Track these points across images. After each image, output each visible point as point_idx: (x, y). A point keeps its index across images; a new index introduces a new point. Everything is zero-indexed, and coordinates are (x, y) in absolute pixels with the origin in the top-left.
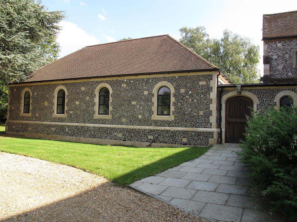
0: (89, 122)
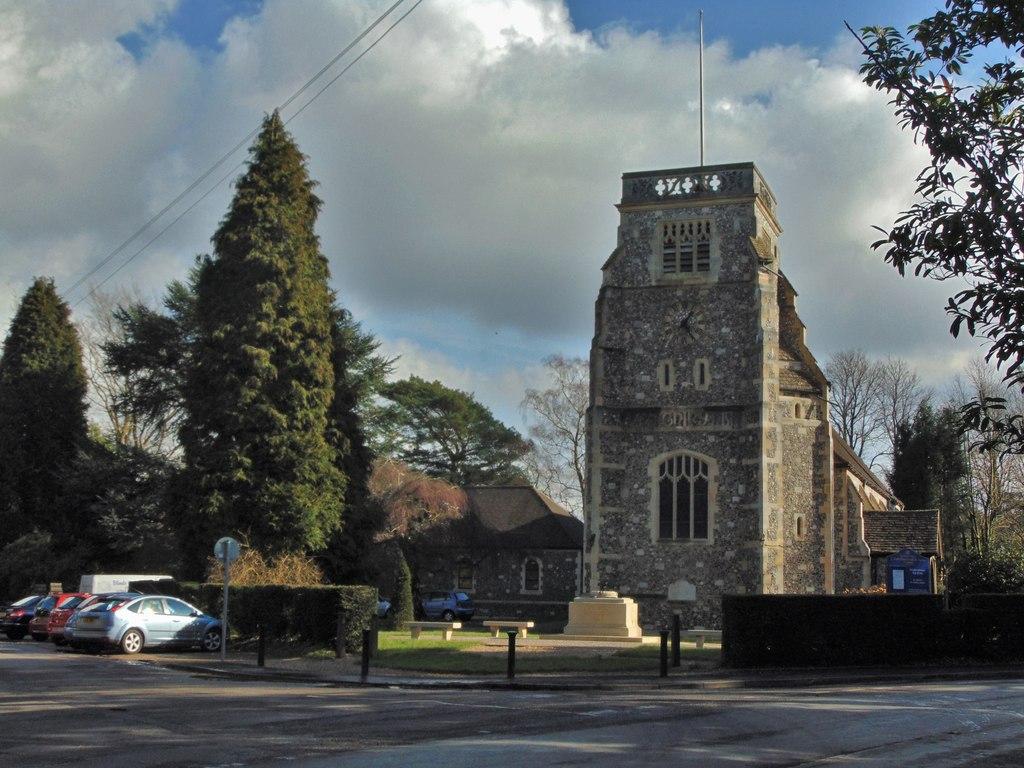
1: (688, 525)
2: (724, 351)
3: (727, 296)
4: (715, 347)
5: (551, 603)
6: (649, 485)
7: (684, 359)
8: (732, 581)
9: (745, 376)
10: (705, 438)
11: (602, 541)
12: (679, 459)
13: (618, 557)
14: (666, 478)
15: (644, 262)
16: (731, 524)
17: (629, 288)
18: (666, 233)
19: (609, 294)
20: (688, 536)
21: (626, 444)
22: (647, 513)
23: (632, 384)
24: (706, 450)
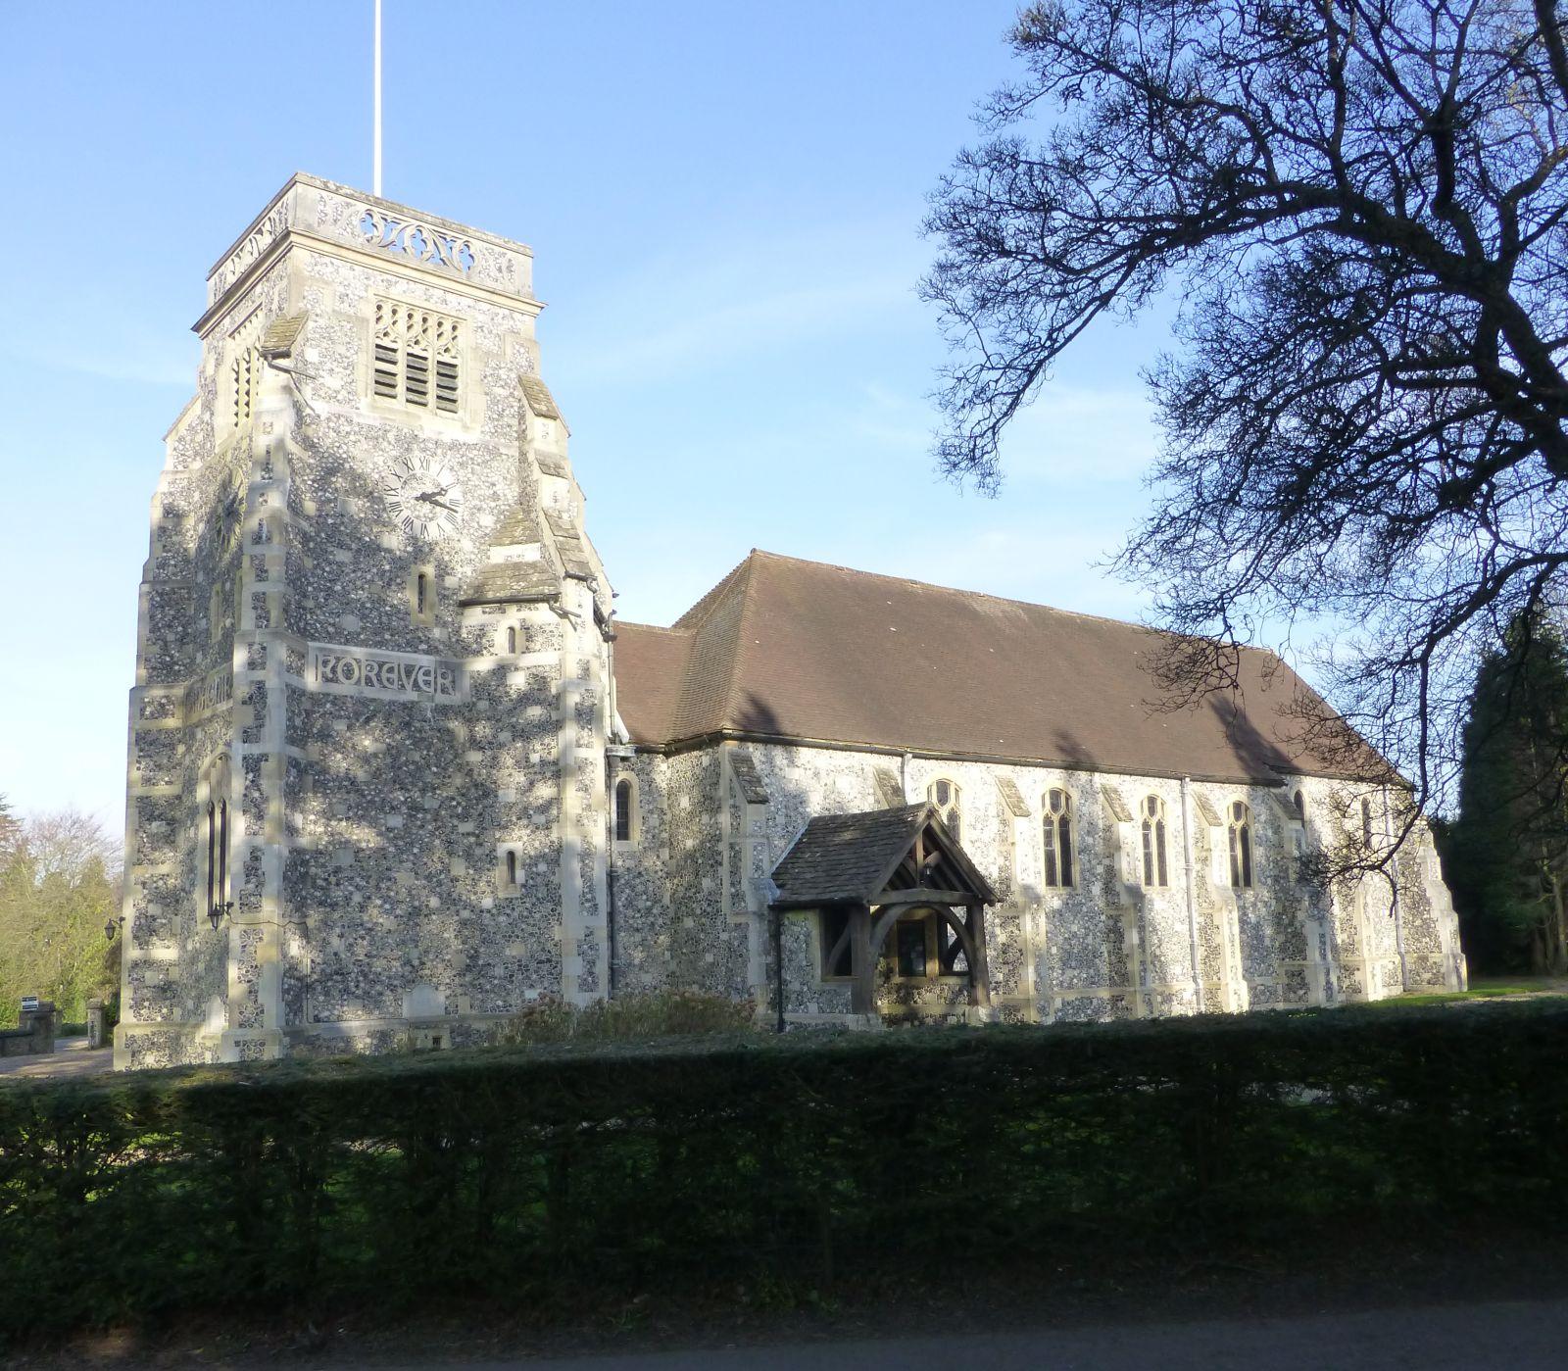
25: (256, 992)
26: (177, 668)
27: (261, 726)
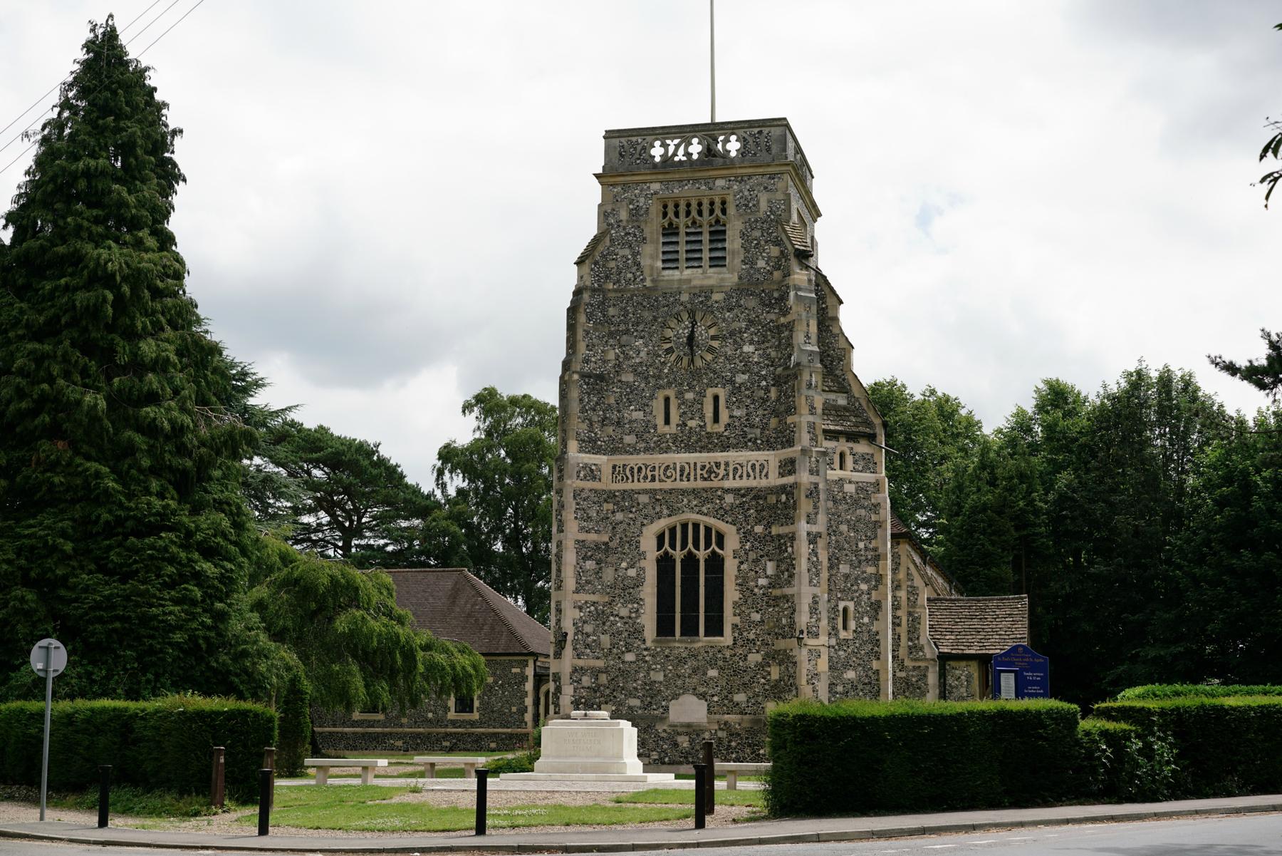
0: (344, 724)
1: (698, 617)
2: (746, 377)
3: (752, 302)
4: (734, 372)
5: (491, 730)
6: (643, 563)
7: (691, 388)
8: (758, 696)
9: (775, 413)
10: (721, 498)
11: (575, 641)
12: (685, 526)
13: (600, 664)
14: (666, 553)
15: (635, 254)
16: (756, 617)
17: (615, 291)
18: (665, 215)
19: (586, 296)
20: (697, 634)
21: (611, 506)
22: (639, 601)
23: (618, 423)
24: (721, 513)
25: (817, 691)
26: (599, 443)
27: (816, 514)
